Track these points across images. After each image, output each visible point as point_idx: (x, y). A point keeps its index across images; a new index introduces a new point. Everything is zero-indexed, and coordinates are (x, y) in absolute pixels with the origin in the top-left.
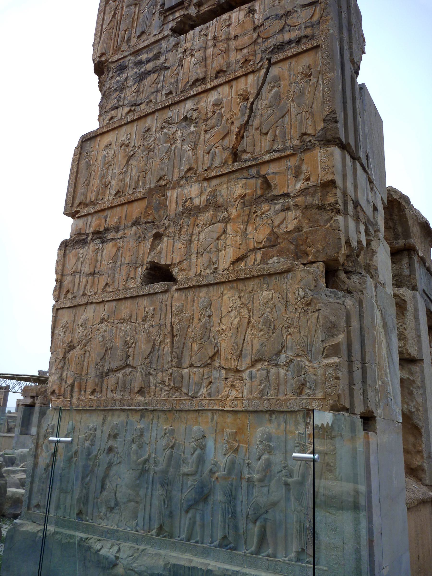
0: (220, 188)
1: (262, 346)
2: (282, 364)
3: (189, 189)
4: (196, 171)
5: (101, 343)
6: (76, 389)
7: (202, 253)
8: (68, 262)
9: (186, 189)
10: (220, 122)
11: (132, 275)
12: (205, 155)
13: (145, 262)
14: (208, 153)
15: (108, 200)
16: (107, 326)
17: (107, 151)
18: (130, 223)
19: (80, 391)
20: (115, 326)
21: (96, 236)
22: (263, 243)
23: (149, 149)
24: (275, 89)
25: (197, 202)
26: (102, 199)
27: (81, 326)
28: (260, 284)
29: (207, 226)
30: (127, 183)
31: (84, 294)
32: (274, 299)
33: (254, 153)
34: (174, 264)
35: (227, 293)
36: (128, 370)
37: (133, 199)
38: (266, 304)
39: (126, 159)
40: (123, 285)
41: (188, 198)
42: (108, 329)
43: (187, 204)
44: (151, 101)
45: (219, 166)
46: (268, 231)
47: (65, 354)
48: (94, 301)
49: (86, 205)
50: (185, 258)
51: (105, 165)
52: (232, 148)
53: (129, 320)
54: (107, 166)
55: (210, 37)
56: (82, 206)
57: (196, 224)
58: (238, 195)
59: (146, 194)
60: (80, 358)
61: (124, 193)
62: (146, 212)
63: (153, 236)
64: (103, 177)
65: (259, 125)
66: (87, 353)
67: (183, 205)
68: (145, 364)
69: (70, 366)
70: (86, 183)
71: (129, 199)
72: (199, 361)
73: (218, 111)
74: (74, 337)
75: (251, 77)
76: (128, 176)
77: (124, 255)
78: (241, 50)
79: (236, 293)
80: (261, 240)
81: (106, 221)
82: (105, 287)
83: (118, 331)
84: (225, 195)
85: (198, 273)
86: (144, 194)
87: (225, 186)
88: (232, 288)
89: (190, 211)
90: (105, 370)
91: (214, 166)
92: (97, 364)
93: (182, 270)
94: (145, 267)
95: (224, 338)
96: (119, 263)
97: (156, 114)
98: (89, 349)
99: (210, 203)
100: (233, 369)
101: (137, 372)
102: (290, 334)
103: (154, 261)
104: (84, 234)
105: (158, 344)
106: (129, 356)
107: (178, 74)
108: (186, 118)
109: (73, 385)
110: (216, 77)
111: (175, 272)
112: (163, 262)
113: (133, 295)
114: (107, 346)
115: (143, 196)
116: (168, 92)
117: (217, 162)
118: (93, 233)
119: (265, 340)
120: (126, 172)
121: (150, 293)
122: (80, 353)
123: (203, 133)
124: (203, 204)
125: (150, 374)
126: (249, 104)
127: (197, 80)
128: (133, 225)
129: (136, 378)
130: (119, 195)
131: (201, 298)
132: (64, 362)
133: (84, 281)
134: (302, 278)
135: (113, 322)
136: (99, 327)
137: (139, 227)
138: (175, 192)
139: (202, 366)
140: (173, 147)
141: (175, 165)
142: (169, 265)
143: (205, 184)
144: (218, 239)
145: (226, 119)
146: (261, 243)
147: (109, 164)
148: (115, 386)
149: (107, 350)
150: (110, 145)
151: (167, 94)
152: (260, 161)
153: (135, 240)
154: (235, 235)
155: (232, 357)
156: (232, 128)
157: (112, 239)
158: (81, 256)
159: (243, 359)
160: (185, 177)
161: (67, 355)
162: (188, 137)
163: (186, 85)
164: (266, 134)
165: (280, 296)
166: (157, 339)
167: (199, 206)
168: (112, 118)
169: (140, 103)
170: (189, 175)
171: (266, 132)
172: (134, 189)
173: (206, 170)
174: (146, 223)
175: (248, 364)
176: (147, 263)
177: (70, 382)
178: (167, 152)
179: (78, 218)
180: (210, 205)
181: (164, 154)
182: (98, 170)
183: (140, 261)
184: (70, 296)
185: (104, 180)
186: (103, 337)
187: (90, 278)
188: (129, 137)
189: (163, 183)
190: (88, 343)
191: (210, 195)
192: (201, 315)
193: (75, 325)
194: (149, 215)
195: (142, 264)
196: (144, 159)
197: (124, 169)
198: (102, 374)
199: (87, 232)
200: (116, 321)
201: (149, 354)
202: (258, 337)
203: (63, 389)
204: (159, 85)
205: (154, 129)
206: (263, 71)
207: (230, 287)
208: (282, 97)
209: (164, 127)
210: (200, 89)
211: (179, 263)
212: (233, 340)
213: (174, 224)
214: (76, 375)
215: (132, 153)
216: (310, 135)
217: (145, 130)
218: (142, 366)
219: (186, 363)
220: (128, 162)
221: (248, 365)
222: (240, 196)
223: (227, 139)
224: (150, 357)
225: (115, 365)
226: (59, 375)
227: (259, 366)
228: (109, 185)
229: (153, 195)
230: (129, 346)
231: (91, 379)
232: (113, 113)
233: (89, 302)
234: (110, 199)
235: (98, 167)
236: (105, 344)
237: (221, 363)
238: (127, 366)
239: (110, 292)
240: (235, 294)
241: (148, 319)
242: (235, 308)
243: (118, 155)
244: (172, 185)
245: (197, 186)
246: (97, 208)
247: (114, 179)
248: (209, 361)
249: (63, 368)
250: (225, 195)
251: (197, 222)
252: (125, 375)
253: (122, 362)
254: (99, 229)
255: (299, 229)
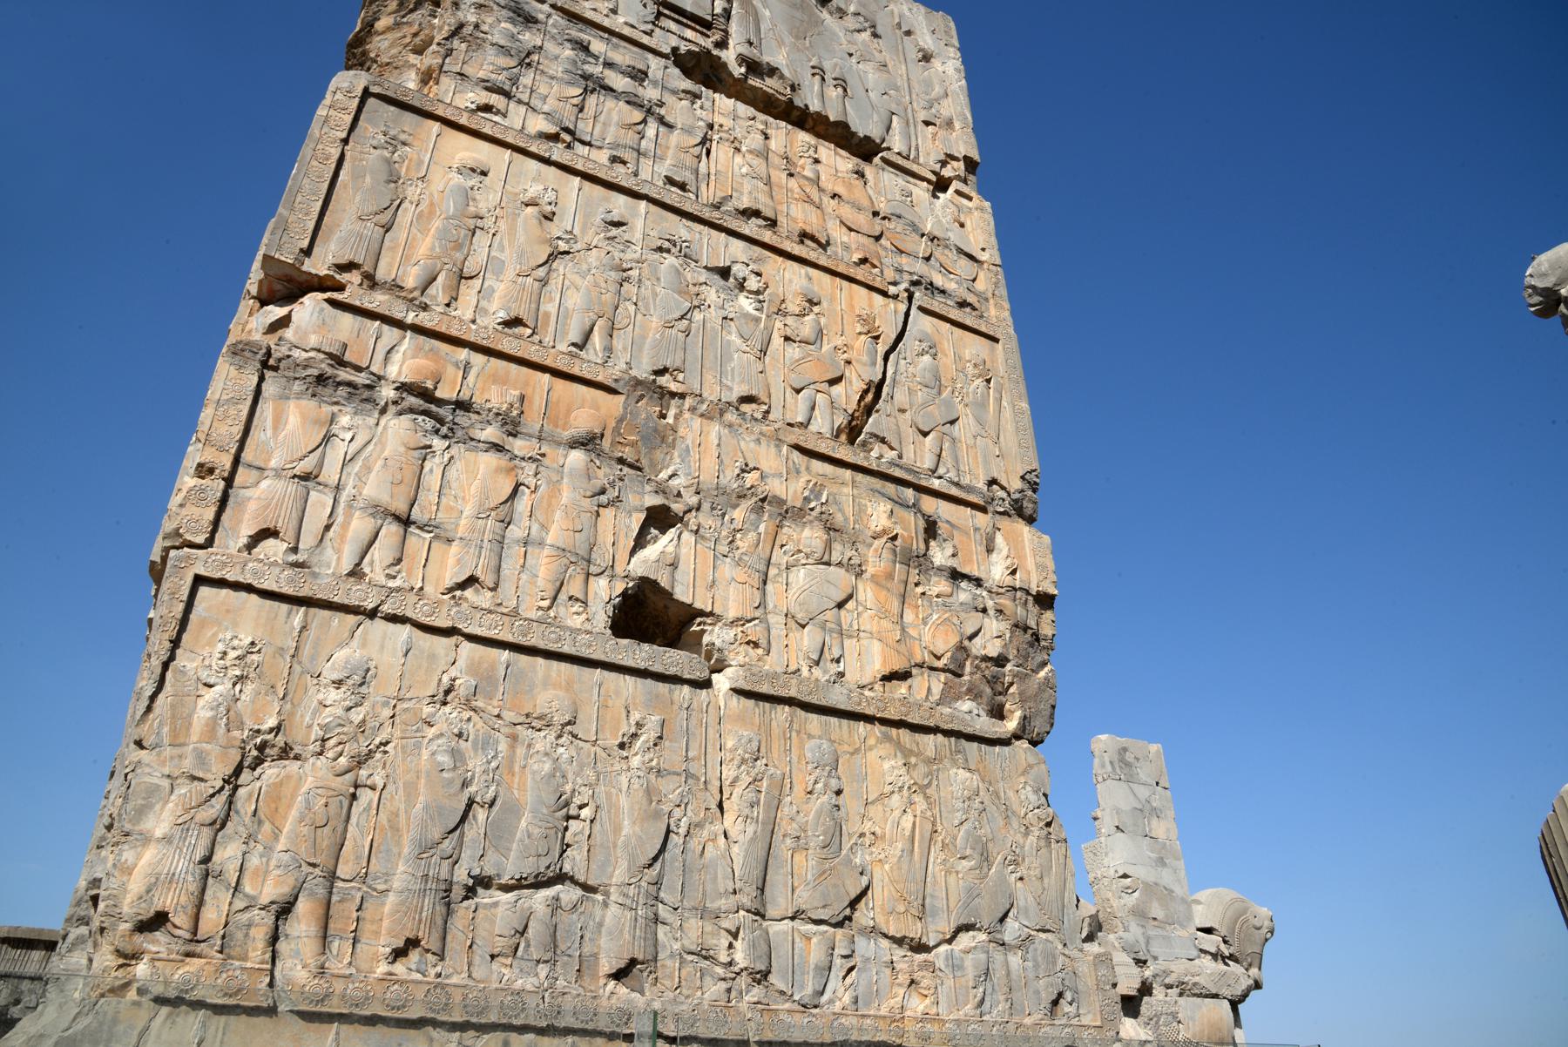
0: (835, 489)
1: (972, 894)
2: (1013, 943)
3: (752, 445)
4: (768, 412)
5: (445, 774)
6: (302, 926)
7: (804, 623)
8: (269, 424)
9: (744, 439)
10: (819, 341)
11: (574, 588)
12: (789, 390)
13: (619, 570)
14: (798, 391)
15: (474, 322)
16: (469, 719)
17: (471, 183)
18: (567, 434)
19: (324, 937)
20: (505, 730)
21: (412, 401)
22: (944, 661)
23: (625, 274)
24: (927, 358)
25: (776, 487)
26: (448, 305)
27: (338, 683)
28: (951, 751)
29: (810, 561)
30: (547, 315)
31: (356, 573)
32: (981, 793)
33: (900, 457)
34: (718, 618)
35: (876, 746)
36: (568, 893)
37: (576, 371)
38: (969, 799)
39: (549, 250)
40: (540, 608)
41: (751, 465)
42: (472, 731)
43: (751, 478)
44: (624, 163)
45: (828, 436)
46: (953, 640)
47: (238, 771)
48: (409, 614)
49: (371, 281)
50: (757, 615)
51: (462, 214)
52: (852, 415)
53: (569, 727)
54: (471, 223)
55: (773, 144)
56: (354, 278)
57: (778, 543)
58: (879, 529)
59: (622, 382)
60: (333, 808)
61: (536, 338)
62: (616, 430)
63: (649, 509)
64: (458, 246)
65: (907, 407)
66: (366, 796)
67: (738, 475)
68: (643, 884)
69: (267, 827)
70: (384, 218)
71: (561, 364)
72: (824, 907)
73: (812, 316)
74: (292, 714)
75: (878, 298)
76: (551, 300)
77: (538, 514)
78: (851, 230)
79: (899, 754)
80: (942, 652)
81: (464, 378)
82: (463, 586)
83: (521, 751)
84: (849, 510)
85: (792, 668)
86: (616, 380)
87: (847, 490)
88: (887, 738)
89: (763, 500)
90: (461, 875)
91: (813, 428)
92: (425, 848)
93: (748, 643)
94: (620, 587)
95: (881, 857)
96: (515, 532)
97: (643, 204)
98: (378, 780)
99: (812, 509)
100: (912, 939)
101: (605, 904)
102: (1021, 879)
103: (654, 583)
104: (358, 369)
105: (682, 831)
106: (568, 846)
107: (699, 157)
108: (724, 273)
109: (285, 909)
110: (802, 242)
111: (715, 636)
112: (682, 594)
113: (585, 652)
114: (472, 789)
115: (613, 385)
116: (677, 179)
117: (822, 423)
118: (403, 387)
119: (976, 881)
120: (544, 282)
121: (651, 668)
122: (333, 785)
123: (777, 341)
124: (793, 501)
125: (656, 919)
126: (882, 348)
127: (756, 214)
128: (575, 444)
129: (600, 925)
130: (519, 330)
131: (810, 736)
132: (231, 803)
133: (360, 525)
134: (1030, 766)
135: (498, 716)
136: (434, 715)
137: (598, 463)
138: (714, 429)
139: (833, 921)
140: (698, 316)
141: (707, 364)
142: (702, 613)
143: (796, 455)
144: (840, 605)
145: (832, 345)
146: (938, 658)
147: (480, 223)
148: (515, 940)
149: (471, 803)
150: (484, 174)
151: (670, 181)
152: (924, 483)
153: (589, 494)
154: (883, 616)
155: (907, 910)
156: (850, 373)
157: (498, 448)
158: (348, 436)
159: (930, 919)
160: (737, 409)
161: (245, 776)
162: (743, 321)
163: (724, 198)
164: (925, 434)
165: (991, 789)
166: (678, 813)
167: (784, 502)
168: (487, 108)
169: (587, 139)
170: (746, 408)
171: (927, 430)
172: (574, 344)
173: (790, 425)
174: (621, 461)
175: (943, 933)
176: (627, 577)
177: (271, 890)
178: (682, 317)
179: (334, 303)
180: (813, 513)
181: (677, 315)
182: (431, 213)
183: (601, 558)
184: (270, 546)
185: (459, 256)
186: (455, 753)
187: (391, 530)
188: (550, 196)
189: (664, 380)
190: (370, 755)
191: (812, 491)
192: (816, 782)
193: (297, 668)
194: (626, 445)
195: (609, 571)
196: (613, 288)
197: (541, 272)
198: (448, 891)
199: (374, 369)
200: (509, 716)
201: (655, 859)
202: (957, 873)
203: (212, 918)
204: (644, 143)
205: (638, 235)
206: (903, 307)
207: (880, 732)
208: (943, 382)
209: (668, 251)
210: (767, 236)
211: (739, 619)
212: (905, 867)
213: (713, 509)
214: (306, 869)
215: (563, 246)
216: (1003, 488)
217: (609, 218)
218: (632, 891)
219: (779, 903)
220: (553, 256)
221: (941, 936)
222: (884, 532)
223: (838, 390)
224: (658, 866)
225: (511, 866)
226: (199, 854)
227: (965, 940)
228: (477, 283)
229: (642, 397)
230: (573, 812)
231: (391, 898)
232: (496, 100)
233: (385, 608)
234: (478, 321)
235: (432, 204)
236: (465, 784)
237: (877, 920)
238: (561, 878)
239: (490, 612)
240: (896, 755)
241: (638, 744)
242: (901, 788)
243: (514, 220)
244: (704, 407)
245: (773, 450)
246: (425, 319)
247: (498, 273)
248: (848, 911)
249: (220, 824)
250: (849, 510)
251: (781, 539)
252: (555, 905)
253: (544, 862)
254: (436, 388)
255: (1000, 661)
